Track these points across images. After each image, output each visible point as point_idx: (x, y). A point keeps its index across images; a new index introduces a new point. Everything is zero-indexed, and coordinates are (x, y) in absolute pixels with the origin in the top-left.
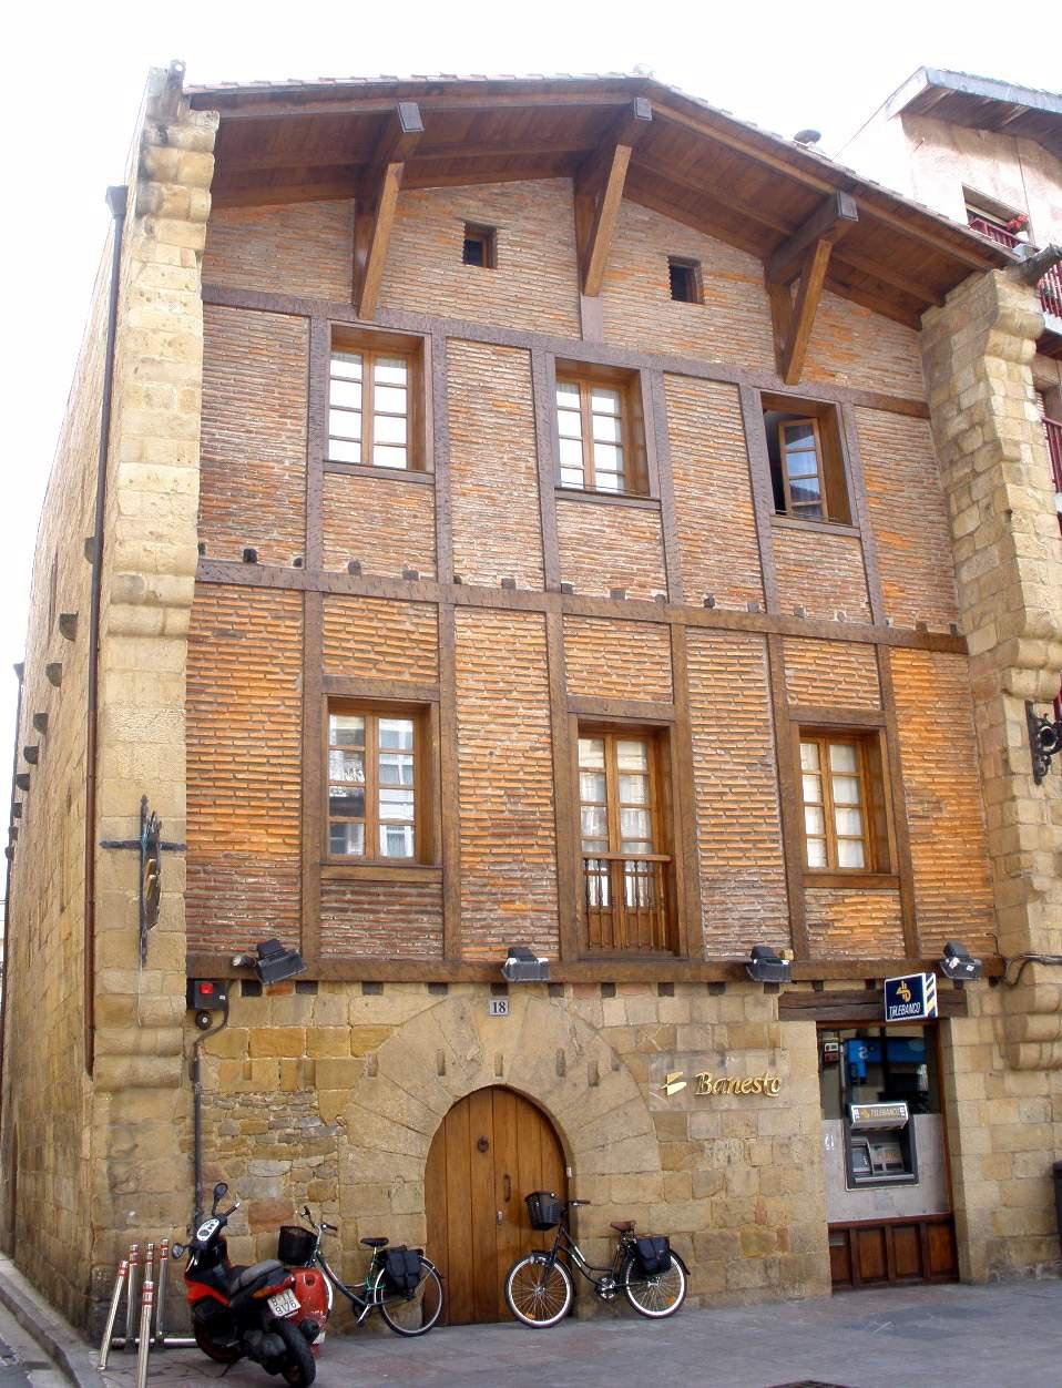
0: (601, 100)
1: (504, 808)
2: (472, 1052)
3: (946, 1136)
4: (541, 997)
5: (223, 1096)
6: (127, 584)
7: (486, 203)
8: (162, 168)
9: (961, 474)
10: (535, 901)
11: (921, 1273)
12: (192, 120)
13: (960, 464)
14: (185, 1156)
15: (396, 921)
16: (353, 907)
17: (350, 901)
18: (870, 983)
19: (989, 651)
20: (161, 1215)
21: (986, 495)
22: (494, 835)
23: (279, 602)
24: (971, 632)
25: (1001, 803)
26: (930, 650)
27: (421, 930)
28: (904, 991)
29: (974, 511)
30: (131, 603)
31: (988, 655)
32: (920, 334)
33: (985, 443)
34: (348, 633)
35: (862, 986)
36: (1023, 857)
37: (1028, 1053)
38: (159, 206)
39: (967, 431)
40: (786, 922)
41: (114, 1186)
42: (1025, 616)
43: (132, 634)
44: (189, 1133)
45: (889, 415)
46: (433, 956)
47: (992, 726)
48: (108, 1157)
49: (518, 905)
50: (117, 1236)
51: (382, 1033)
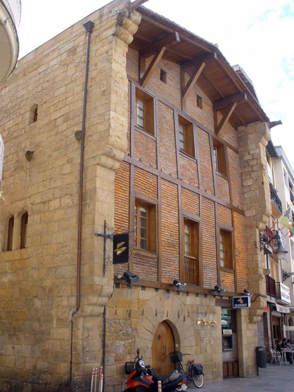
0: (207, 49)
1: (170, 239)
2: (162, 310)
3: (237, 339)
4: (175, 295)
5: (110, 320)
6: (110, 150)
7: (164, 65)
8: (126, 24)
9: (248, 170)
10: (175, 267)
11: (233, 375)
12: (136, 13)
13: (247, 167)
14: (100, 339)
15: (148, 269)
16: (139, 263)
17: (138, 261)
18: (230, 297)
19: (252, 216)
20: (95, 359)
21: (256, 177)
22: (167, 246)
23: (125, 166)
24: (247, 210)
25: (252, 255)
26: (239, 213)
27: (152, 272)
28: (241, 301)
29: (251, 180)
30: (107, 156)
31: (252, 217)
32: (237, 132)
33: (257, 164)
34: (139, 179)
35: (228, 298)
36: (259, 269)
37: (255, 318)
38: (120, 35)
39: (250, 159)
40: (217, 279)
41: (83, 349)
42: (266, 209)
43: (104, 166)
44: (102, 331)
45: (232, 151)
46: (155, 280)
47: (251, 235)
48: (82, 339)
49: (172, 267)
50: (84, 366)
51: (145, 301)
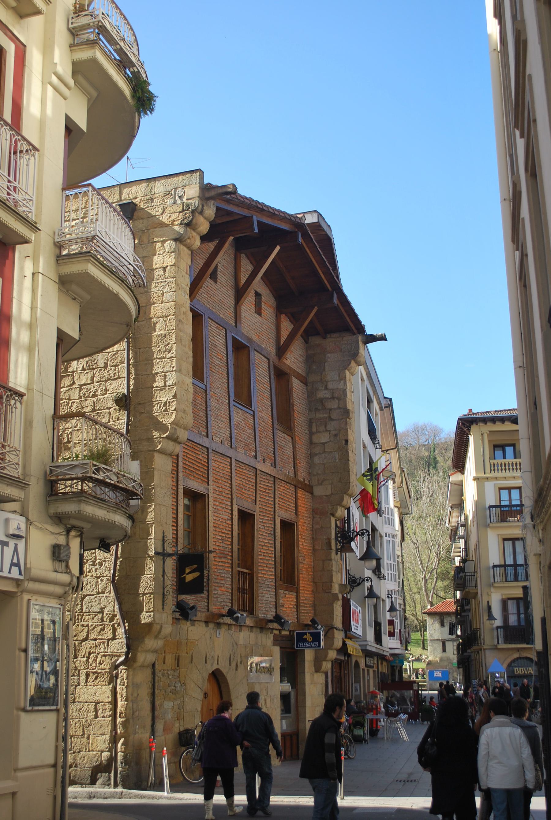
9: (322, 416)
19: (326, 496)
28: (308, 637)
29: (327, 434)
33: (339, 408)
45: (298, 381)
47: (322, 527)
